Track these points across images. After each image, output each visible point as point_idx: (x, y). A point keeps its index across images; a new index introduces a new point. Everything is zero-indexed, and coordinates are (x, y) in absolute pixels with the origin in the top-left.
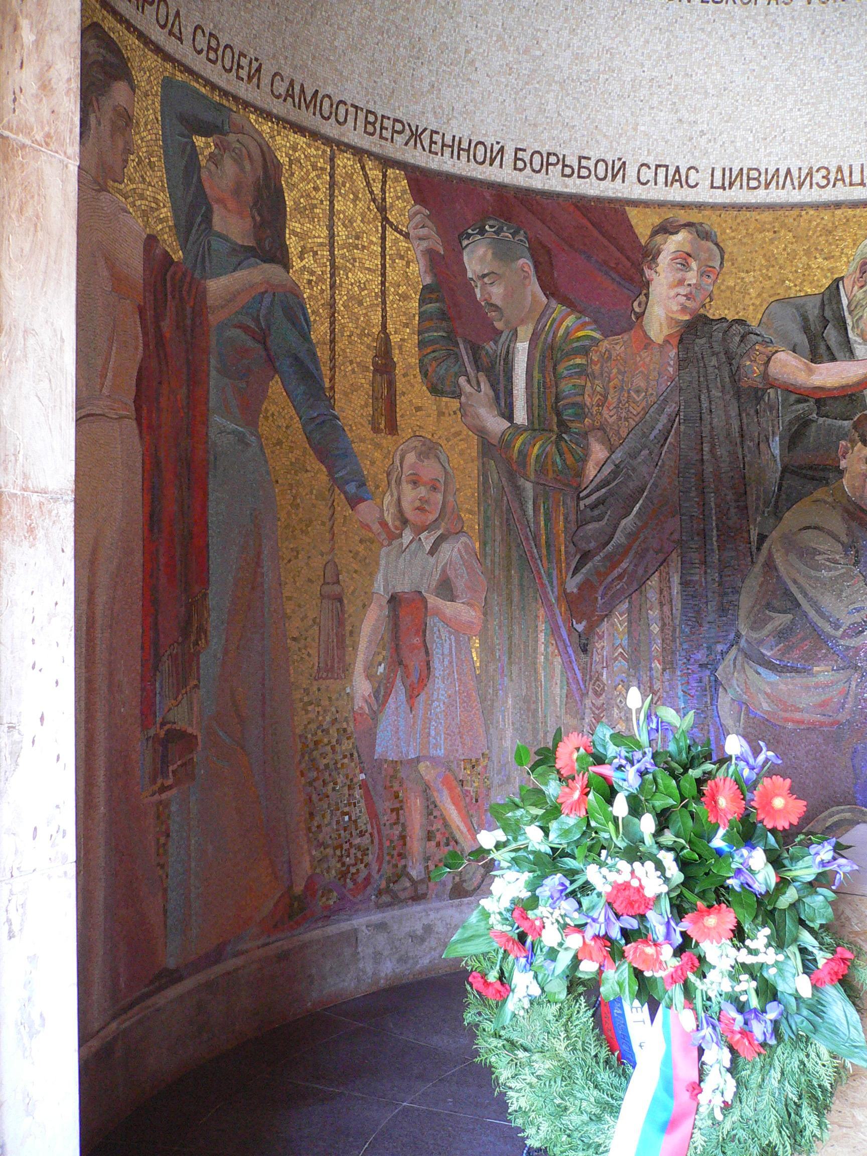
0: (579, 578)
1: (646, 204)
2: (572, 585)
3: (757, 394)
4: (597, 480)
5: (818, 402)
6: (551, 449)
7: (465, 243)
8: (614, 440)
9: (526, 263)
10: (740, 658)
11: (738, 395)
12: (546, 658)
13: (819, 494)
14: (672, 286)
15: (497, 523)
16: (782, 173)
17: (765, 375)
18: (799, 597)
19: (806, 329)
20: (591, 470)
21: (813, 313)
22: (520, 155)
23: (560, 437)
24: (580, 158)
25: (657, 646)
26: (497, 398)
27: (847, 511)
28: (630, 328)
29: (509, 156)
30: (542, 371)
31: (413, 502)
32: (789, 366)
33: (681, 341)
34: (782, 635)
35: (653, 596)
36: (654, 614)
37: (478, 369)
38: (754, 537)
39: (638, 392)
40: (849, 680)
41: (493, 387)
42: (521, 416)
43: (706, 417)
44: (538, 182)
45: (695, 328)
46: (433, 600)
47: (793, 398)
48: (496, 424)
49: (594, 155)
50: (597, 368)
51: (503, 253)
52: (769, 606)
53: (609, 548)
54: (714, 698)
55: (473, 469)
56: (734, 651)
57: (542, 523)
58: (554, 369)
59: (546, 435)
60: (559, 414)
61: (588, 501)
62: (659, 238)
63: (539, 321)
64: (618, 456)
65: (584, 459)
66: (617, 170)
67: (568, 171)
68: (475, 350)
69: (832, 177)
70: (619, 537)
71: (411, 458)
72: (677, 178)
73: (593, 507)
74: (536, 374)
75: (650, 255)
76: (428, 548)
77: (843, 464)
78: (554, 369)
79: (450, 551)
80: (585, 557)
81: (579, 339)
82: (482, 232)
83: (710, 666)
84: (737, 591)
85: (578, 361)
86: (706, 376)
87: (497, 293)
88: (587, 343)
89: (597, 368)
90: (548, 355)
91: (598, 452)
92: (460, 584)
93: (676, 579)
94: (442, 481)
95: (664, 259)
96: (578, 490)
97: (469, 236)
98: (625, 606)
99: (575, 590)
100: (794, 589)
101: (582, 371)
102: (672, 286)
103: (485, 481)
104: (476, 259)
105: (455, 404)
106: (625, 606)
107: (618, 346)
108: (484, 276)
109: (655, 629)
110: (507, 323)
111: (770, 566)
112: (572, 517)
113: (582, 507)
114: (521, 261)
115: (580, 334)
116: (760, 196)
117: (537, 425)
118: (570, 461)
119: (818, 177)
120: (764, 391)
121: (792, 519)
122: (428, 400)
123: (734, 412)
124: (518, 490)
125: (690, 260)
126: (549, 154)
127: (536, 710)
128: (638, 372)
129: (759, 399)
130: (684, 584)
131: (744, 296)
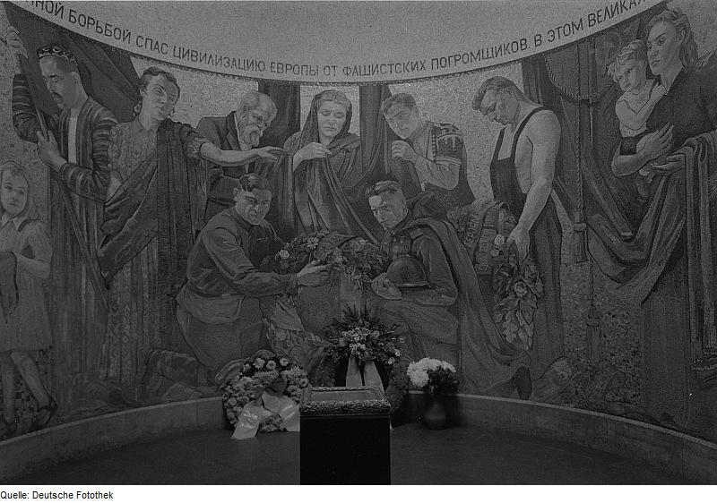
0: (105, 248)
1: (142, 57)
2: (101, 253)
3: (196, 162)
4: (115, 198)
5: (225, 169)
6: (89, 178)
7: (41, 55)
8: (124, 177)
9: (75, 74)
10: (188, 290)
11: (186, 161)
12: (87, 291)
13: (225, 211)
14: (154, 102)
15: (59, 216)
16: (208, 56)
17: (199, 153)
18: (216, 262)
19: (219, 134)
20: (111, 192)
21: (222, 125)
22: (73, 14)
23: (94, 173)
24: (107, 25)
25: (146, 286)
26: (59, 146)
27: (236, 220)
28: (132, 120)
29: (66, 13)
30: (85, 134)
31: (8, 200)
32: (210, 150)
33: (158, 130)
34: (208, 279)
35: (144, 259)
36: (145, 268)
37: (48, 128)
38: (194, 232)
39: (137, 154)
40: (239, 300)
41: (58, 140)
42: (73, 158)
43: (171, 171)
44: (82, 32)
45: (166, 125)
46: (20, 258)
47: (212, 166)
48: (59, 162)
49: (115, 25)
50: (114, 138)
51: (62, 65)
52: (201, 265)
53: (121, 233)
54: (175, 311)
55: (45, 183)
56: (184, 287)
57: (84, 218)
58: (92, 134)
59: (86, 170)
60: (94, 160)
61: (109, 208)
62: (147, 76)
63: (82, 109)
64: (126, 186)
65: (107, 185)
66: (126, 35)
67: (99, 30)
68: (47, 118)
69: (231, 62)
70: (126, 228)
71: (7, 173)
72: (156, 46)
73: (113, 211)
74: (82, 137)
75: (141, 83)
76: (17, 227)
77: (235, 199)
78: (92, 134)
79: (31, 230)
80: (108, 238)
81: (105, 121)
82: (51, 51)
83: (173, 295)
84: (186, 258)
85: (105, 133)
86: (171, 149)
87: (59, 88)
88: (109, 124)
89: (114, 138)
90: (90, 126)
91: (115, 183)
92: (36, 250)
93: (155, 251)
94: (26, 189)
95: (150, 88)
96: (104, 202)
97: (43, 52)
98: (129, 264)
99: (103, 255)
100: (213, 258)
101: (107, 138)
102: (154, 102)
103: (52, 193)
104: (47, 66)
105: (34, 146)
106: (129, 264)
107: (125, 128)
108: (52, 77)
109: (145, 276)
110: (65, 105)
111: (202, 246)
112: (101, 215)
113: (106, 211)
114: (73, 73)
115: (106, 118)
116: (197, 65)
117: (82, 165)
118: (100, 185)
119: (225, 61)
120: (199, 160)
121: (212, 223)
122: (19, 143)
123: (185, 170)
124: (71, 199)
125: (163, 91)
126: (89, 18)
127: (81, 320)
128: (135, 143)
129: (196, 164)
130: (160, 253)
131: (188, 113)
